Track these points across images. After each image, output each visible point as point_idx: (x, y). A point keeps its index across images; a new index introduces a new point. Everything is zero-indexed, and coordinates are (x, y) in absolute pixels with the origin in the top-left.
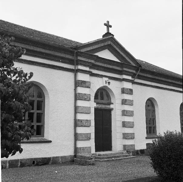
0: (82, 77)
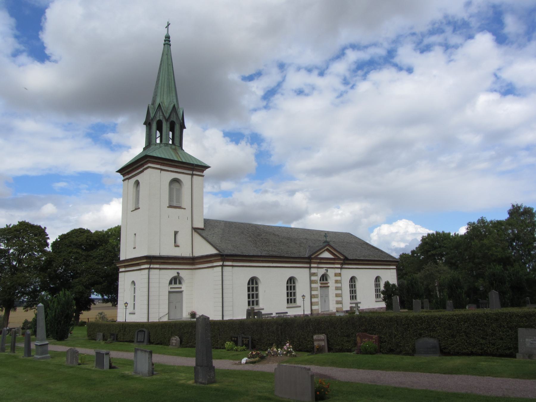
0: (313, 271)
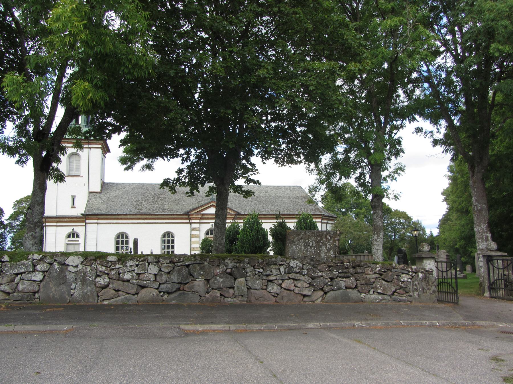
0: (194, 226)
